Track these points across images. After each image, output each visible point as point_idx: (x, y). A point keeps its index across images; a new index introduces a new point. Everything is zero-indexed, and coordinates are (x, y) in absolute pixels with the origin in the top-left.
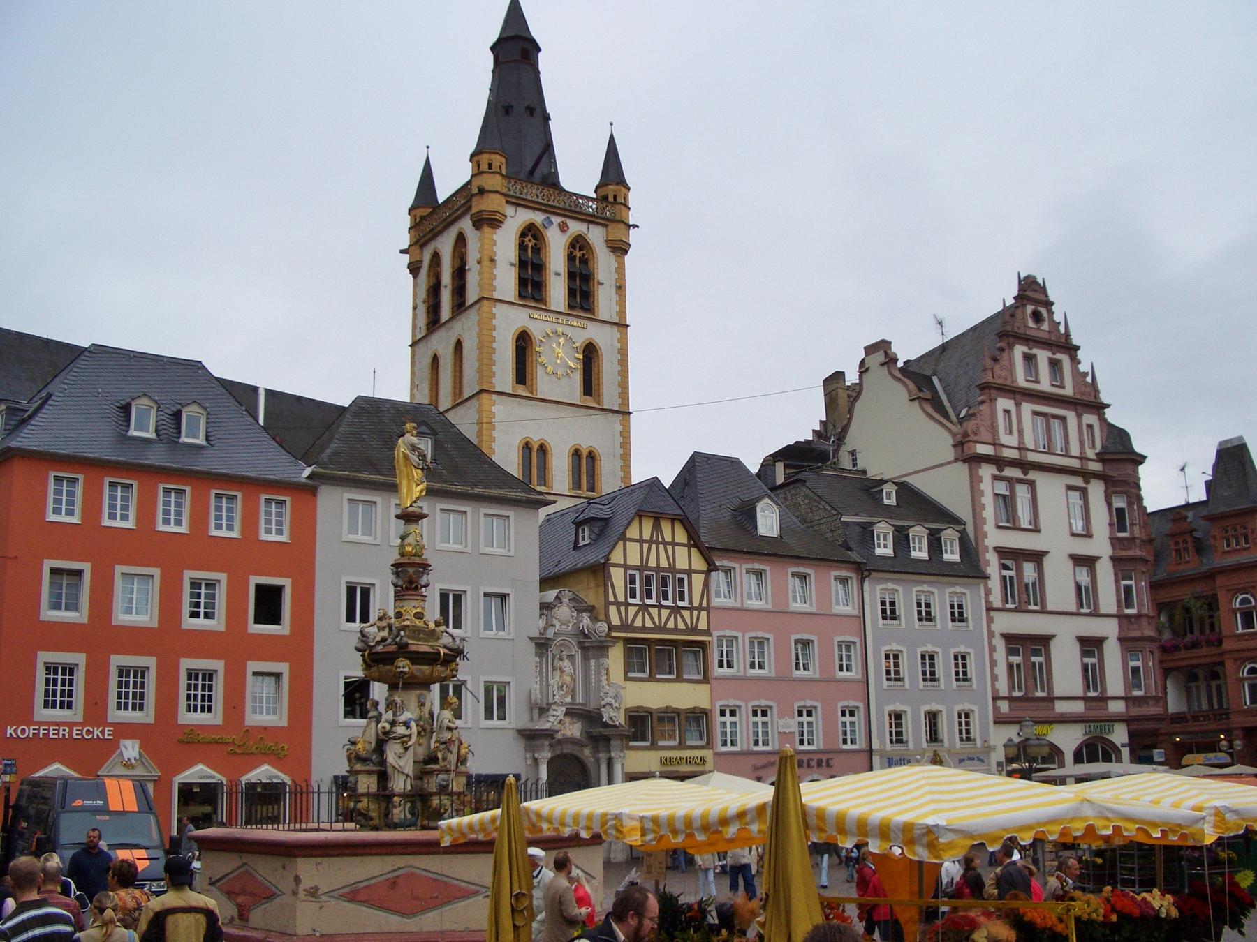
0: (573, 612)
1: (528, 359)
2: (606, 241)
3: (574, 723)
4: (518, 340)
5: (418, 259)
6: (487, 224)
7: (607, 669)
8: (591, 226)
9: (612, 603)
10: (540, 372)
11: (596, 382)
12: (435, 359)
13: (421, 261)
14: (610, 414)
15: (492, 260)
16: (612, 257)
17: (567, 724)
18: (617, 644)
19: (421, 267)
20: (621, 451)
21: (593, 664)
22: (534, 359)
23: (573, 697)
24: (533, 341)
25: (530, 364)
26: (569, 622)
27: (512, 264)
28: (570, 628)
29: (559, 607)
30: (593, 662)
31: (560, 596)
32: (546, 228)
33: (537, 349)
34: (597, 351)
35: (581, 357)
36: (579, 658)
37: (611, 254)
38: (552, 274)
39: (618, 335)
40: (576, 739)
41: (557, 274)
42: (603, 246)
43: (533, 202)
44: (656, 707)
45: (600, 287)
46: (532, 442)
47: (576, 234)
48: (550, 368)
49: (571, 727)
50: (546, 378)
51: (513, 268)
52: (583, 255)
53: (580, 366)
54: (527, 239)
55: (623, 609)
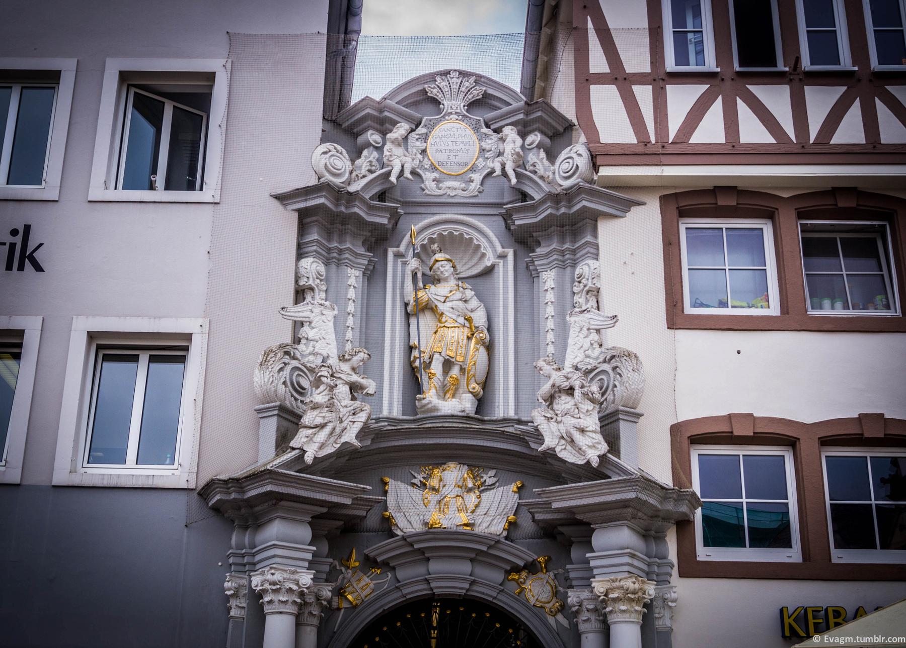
0: (482, 137)
3: (483, 488)
7: (596, 292)
9: (600, 79)
17: (450, 491)
18: (635, 210)
21: (550, 283)
23: (482, 402)
26: (473, 169)
28: (475, 186)
29: (431, 126)
30: (549, 278)
31: (433, 92)
36: (505, 275)
40: (479, 539)
44: (809, 420)
49: (471, 499)
55: (644, 94)
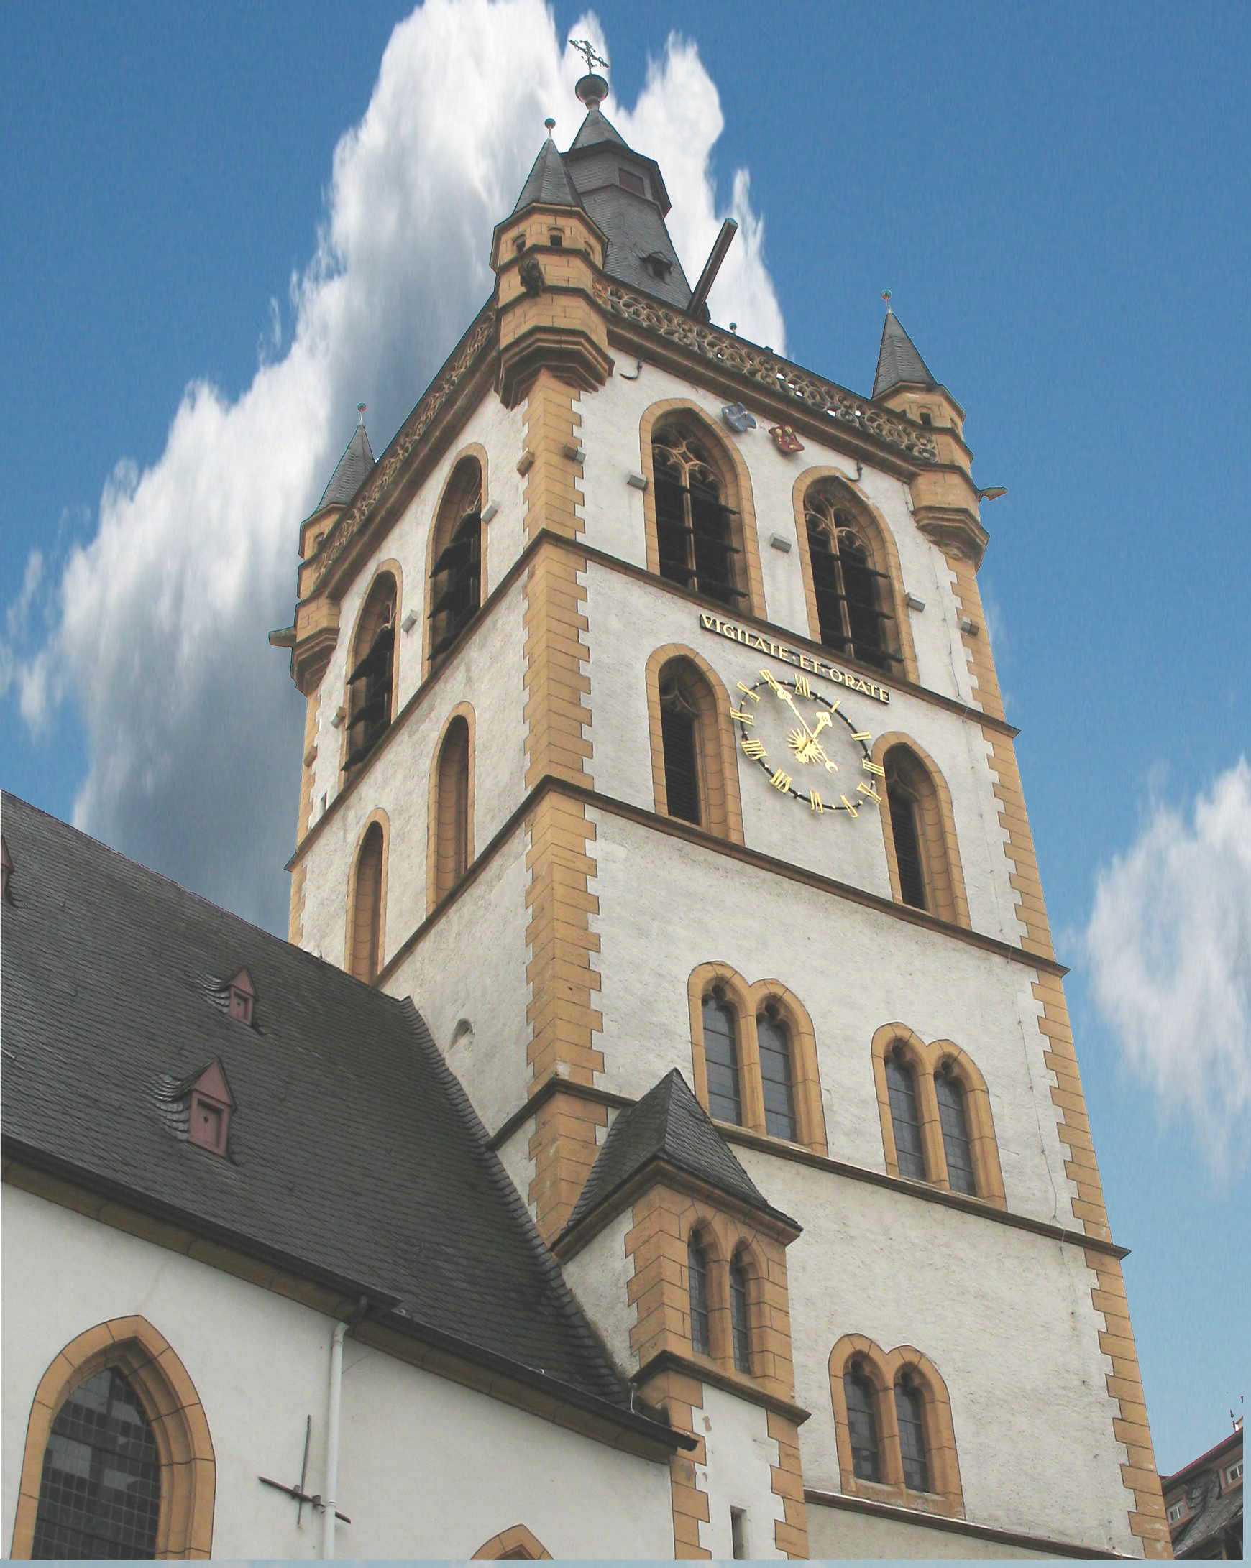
1: (705, 746)
2: (914, 513)
4: (664, 690)
5: (324, 624)
6: (549, 368)
8: (866, 470)
10: (748, 782)
11: (936, 865)
12: (373, 840)
13: (335, 631)
14: (996, 959)
15: (572, 455)
16: (937, 559)
19: (334, 647)
20: (1051, 1079)
22: (725, 739)
24: (719, 693)
25: (712, 766)
27: (634, 483)
32: (735, 431)
33: (735, 714)
34: (933, 790)
35: (881, 771)
37: (935, 549)
38: (764, 546)
39: (988, 748)
41: (780, 546)
42: (910, 525)
43: (685, 351)
45: (914, 615)
46: (736, 981)
47: (826, 473)
48: (780, 775)
50: (770, 803)
51: (639, 494)
52: (850, 537)
53: (879, 797)
54: (675, 451)
